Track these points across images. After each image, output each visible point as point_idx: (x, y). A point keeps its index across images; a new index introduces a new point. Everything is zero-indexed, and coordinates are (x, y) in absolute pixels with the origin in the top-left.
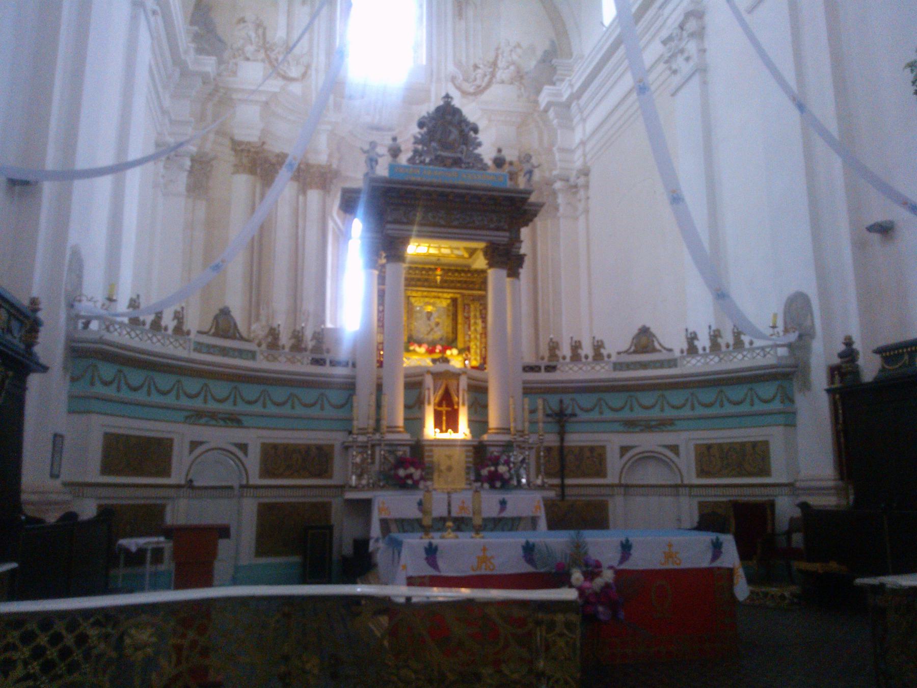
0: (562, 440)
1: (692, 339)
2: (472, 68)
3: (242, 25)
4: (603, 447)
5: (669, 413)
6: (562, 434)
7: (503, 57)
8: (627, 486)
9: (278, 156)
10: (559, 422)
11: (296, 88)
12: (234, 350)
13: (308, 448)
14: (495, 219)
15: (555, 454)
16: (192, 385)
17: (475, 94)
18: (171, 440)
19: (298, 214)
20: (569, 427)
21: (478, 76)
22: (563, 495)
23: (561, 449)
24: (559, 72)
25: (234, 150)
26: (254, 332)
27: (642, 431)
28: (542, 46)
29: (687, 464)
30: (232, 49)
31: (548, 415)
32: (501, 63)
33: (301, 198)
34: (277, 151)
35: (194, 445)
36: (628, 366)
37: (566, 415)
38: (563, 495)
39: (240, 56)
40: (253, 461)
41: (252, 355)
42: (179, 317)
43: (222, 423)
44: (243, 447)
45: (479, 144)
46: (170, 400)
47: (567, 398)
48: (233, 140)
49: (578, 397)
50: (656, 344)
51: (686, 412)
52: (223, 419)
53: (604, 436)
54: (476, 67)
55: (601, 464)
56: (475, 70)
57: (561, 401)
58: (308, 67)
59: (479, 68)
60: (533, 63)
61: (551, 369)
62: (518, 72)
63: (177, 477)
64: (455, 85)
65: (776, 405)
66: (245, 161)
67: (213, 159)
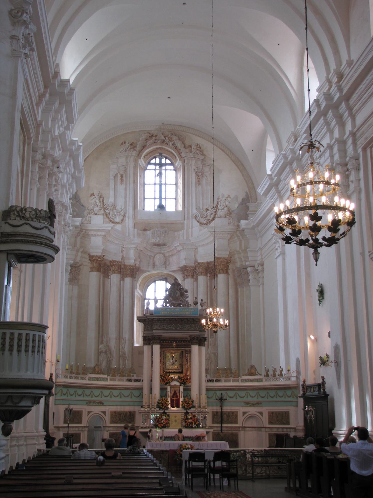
0: (221, 409)
2: (205, 211)
3: (93, 197)
4: (237, 412)
5: (260, 399)
6: (221, 406)
7: (221, 203)
8: (245, 427)
9: (111, 262)
10: (220, 402)
11: (118, 227)
12: (101, 378)
14: (193, 326)
15: (219, 414)
16: (88, 392)
17: (206, 224)
18: (82, 411)
19: (120, 291)
20: (225, 404)
21: (208, 215)
22: (222, 430)
23: (222, 412)
24: (250, 209)
25: (90, 260)
26: (101, 349)
27: (250, 406)
28: (241, 196)
29: (265, 420)
30: (88, 209)
31: (216, 399)
32: (220, 207)
33: (122, 282)
36: (246, 381)
37: (223, 399)
38: (222, 430)
39: (92, 213)
40: (107, 418)
43: (97, 404)
45: (188, 297)
47: (224, 392)
48: (89, 255)
49: (228, 392)
50: (256, 372)
51: (265, 399)
52: (98, 403)
53: (237, 408)
54: (207, 210)
55: (236, 419)
56: (206, 212)
57: (221, 394)
58: (124, 216)
59: (208, 210)
60: (237, 205)
62: (229, 211)
63: (84, 424)
64: (196, 220)
65: (291, 399)
66: (95, 265)
67: (81, 265)
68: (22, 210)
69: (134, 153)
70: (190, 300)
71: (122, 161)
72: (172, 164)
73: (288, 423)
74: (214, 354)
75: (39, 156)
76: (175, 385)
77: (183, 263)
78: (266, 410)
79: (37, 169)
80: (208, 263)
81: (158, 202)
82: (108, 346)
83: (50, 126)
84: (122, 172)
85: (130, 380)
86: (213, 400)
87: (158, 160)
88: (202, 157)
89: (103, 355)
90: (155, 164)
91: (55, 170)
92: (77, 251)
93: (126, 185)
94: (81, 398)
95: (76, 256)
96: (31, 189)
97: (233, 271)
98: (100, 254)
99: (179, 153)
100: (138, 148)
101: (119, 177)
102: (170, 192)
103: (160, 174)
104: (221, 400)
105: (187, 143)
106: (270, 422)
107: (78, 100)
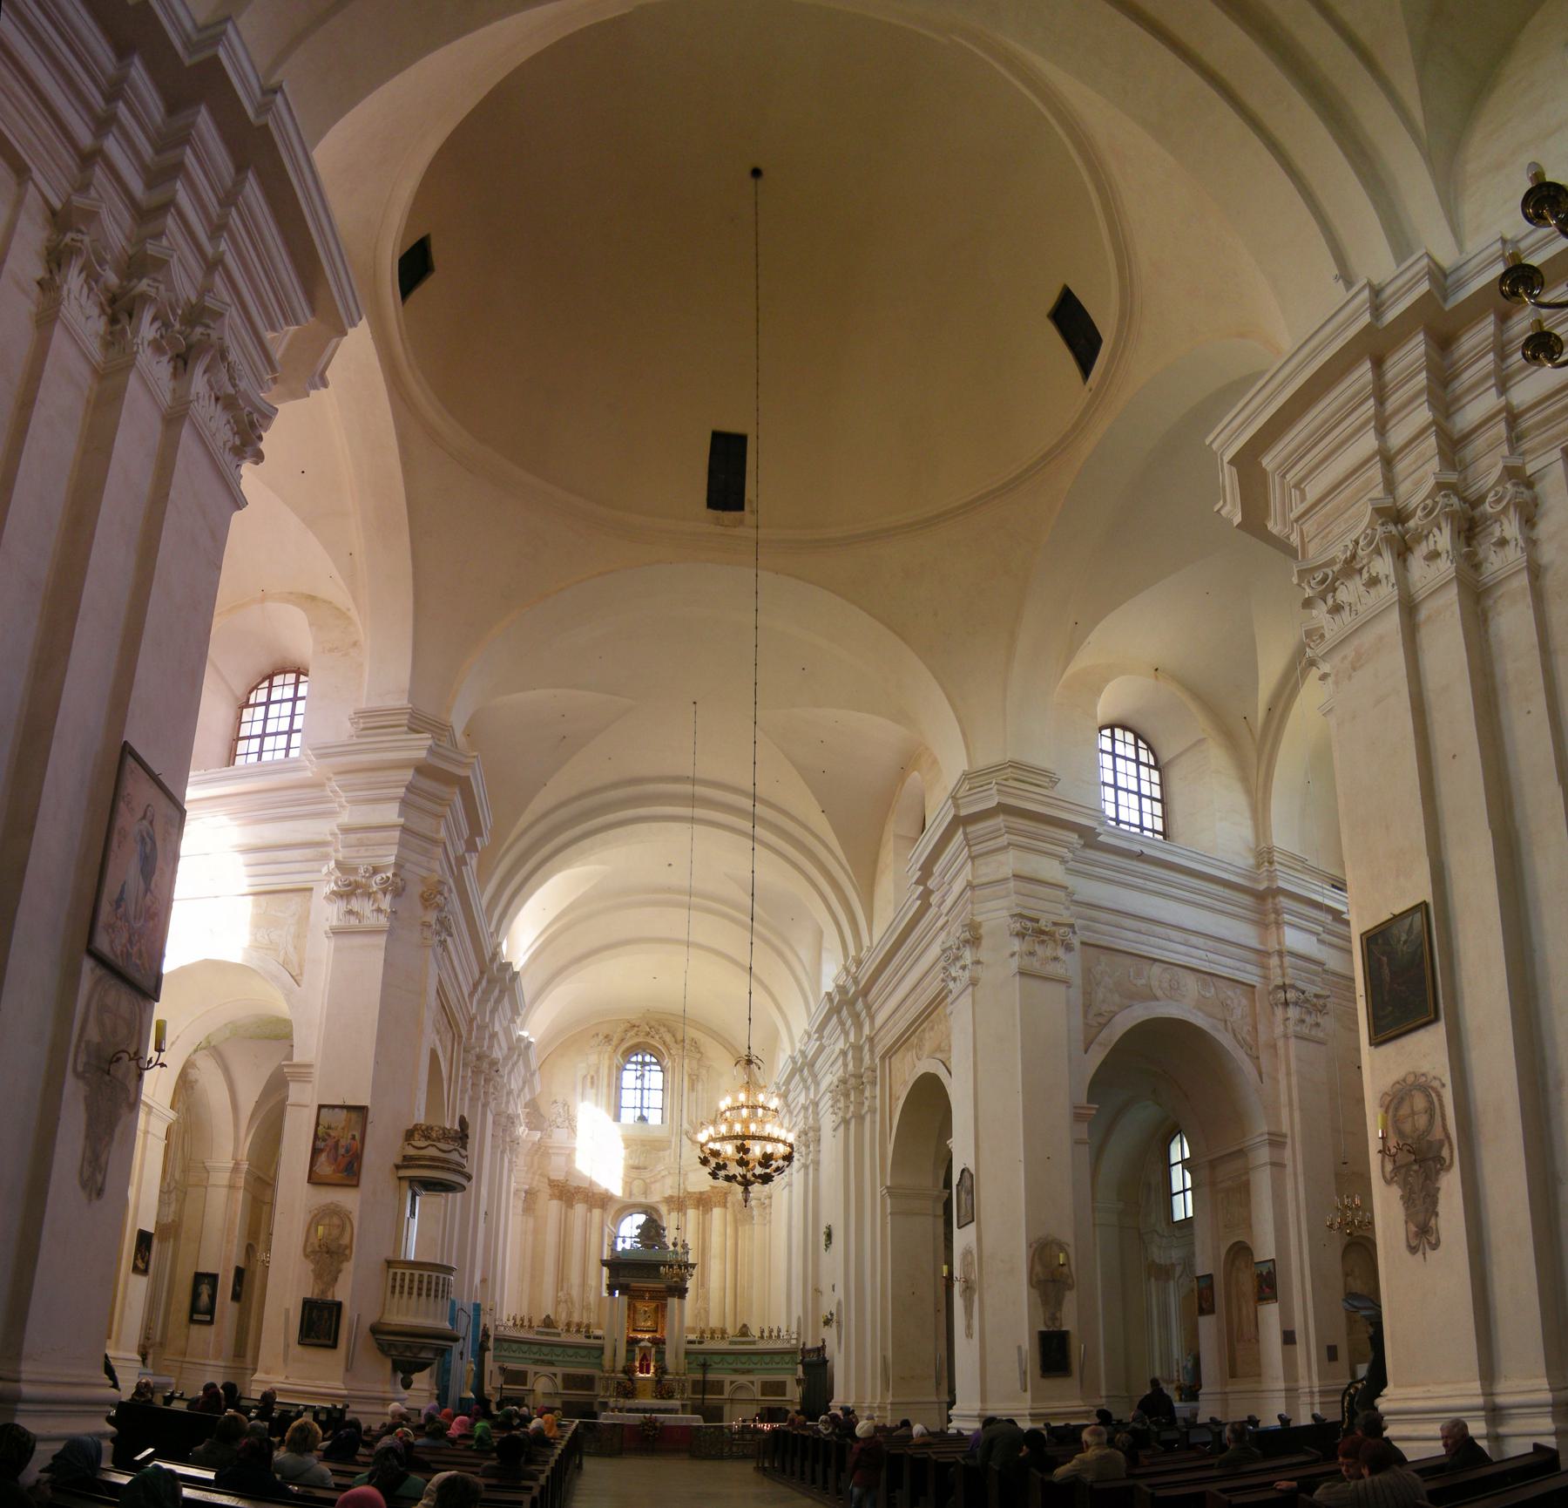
1: (762, 1332)
5: (752, 1366)
6: (704, 1374)
13: (583, 1375)
16: (535, 1349)
19: (586, 1225)
29: (757, 1389)
34: (575, 1185)
35: (536, 1373)
36: (736, 1343)
40: (559, 1380)
41: (559, 1335)
42: (530, 1321)
44: (555, 1375)
46: (527, 1355)
47: (707, 1357)
48: (549, 1179)
61: (700, 1343)
65: (789, 1366)
68: (427, 1128)
69: (610, 1049)
70: (669, 1241)
71: (593, 1059)
72: (658, 1063)
73: (784, 1395)
74: (705, 1309)
75: (472, 1057)
76: (645, 1347)
77: (668, 1193)
78: (758, 1378)
79: (470, 1074)
80: (701, 1193)
81: (638, 1112)
82: (569, 1294)
83: (487, 1020)
84: (592, 1073)
85: (588, 1337)
86: (694, 1365)
87: (640, 1058)
88: (698, 1056)
89: (562, 1305)
90: (636, 1063)
91: (493, 1073)
92: (534, 1174)
93: (598, 1087)
94: (527, 1355)
95: (532, 1179)
96: (461, 1099)
97: (733, 1205)
98: (562, 1178)
99: (669, 1049)
100: (615, 1042)
101: (589, 1080)
102: (655, 1099)
103: (643, 1075)
104: (705, 1367)
105: (680, 1037)
106: (763, 1394)
107: (527, 987)
